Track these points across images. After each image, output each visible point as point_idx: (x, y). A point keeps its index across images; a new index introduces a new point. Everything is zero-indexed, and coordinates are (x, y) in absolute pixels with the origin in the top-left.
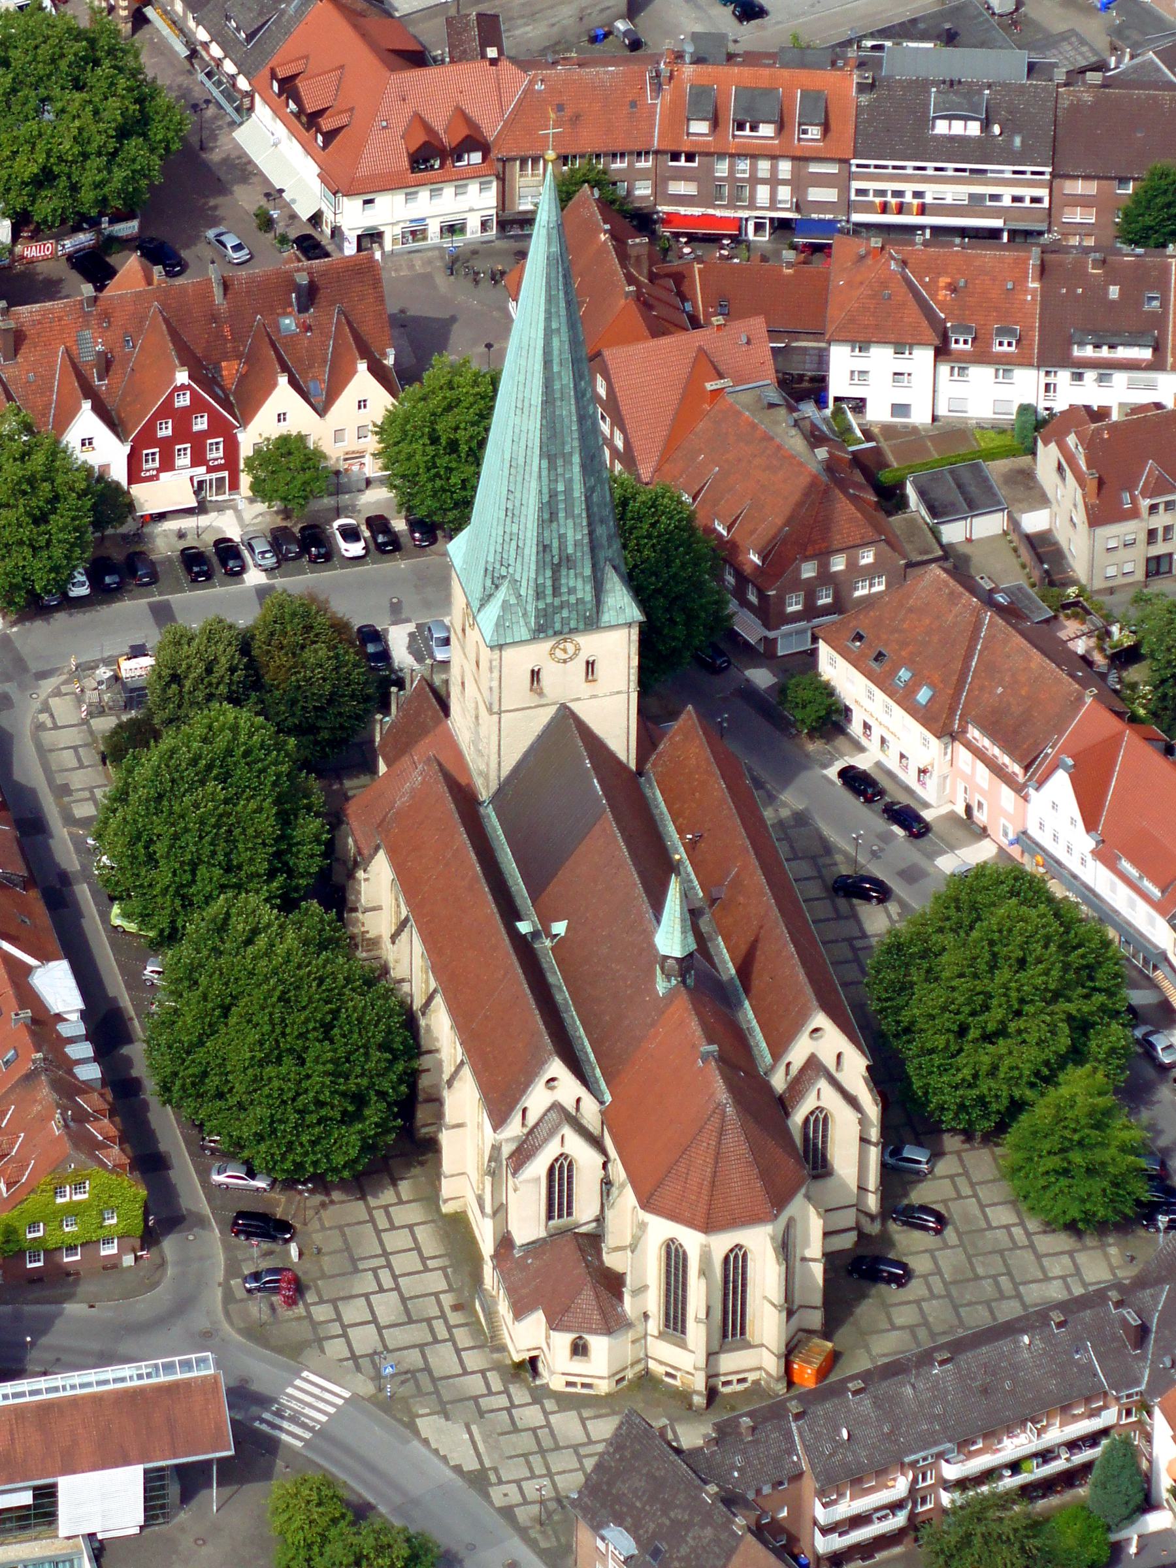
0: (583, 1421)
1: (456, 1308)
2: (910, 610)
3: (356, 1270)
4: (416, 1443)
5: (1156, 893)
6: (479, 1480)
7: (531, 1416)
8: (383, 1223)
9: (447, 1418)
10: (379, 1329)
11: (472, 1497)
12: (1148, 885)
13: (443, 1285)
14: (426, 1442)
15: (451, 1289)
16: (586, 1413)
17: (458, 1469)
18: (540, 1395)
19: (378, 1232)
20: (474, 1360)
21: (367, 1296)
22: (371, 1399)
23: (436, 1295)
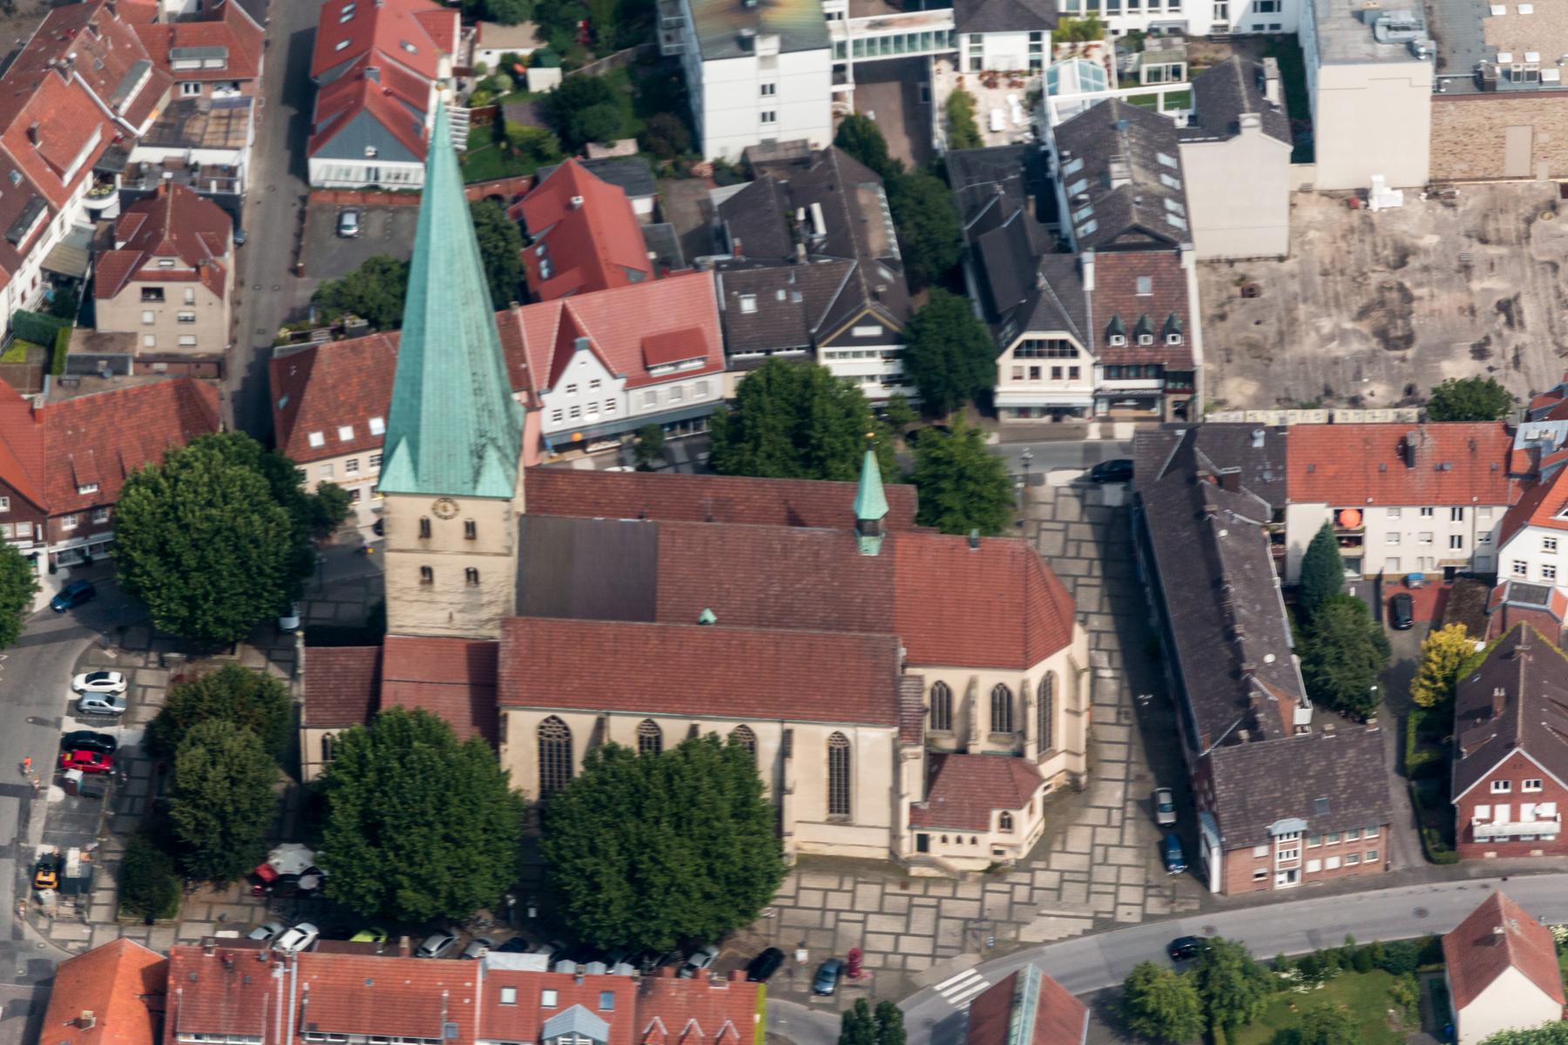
0: (1064, 851)
1: (904, 886)
2: (334, 387)
3: (834, 930)
4: (1047, 948)
5: (698, 364)
6: (1103, 924)
7: (1044, 879)
8: (790, 902)
9: (1027, 923)
10: (906, 934)
11: (1119, 935)
12: (686, 366)
13: (875, 890)
14: (1047, 942)
15: (883, 884)
16: (1057, 847)
17: (1086, 933)
18: (1023, 866)
19: (795, 907)
20: (970, 890)
21: (865, 932)
22: (985, 959)
23: (883, 894)
